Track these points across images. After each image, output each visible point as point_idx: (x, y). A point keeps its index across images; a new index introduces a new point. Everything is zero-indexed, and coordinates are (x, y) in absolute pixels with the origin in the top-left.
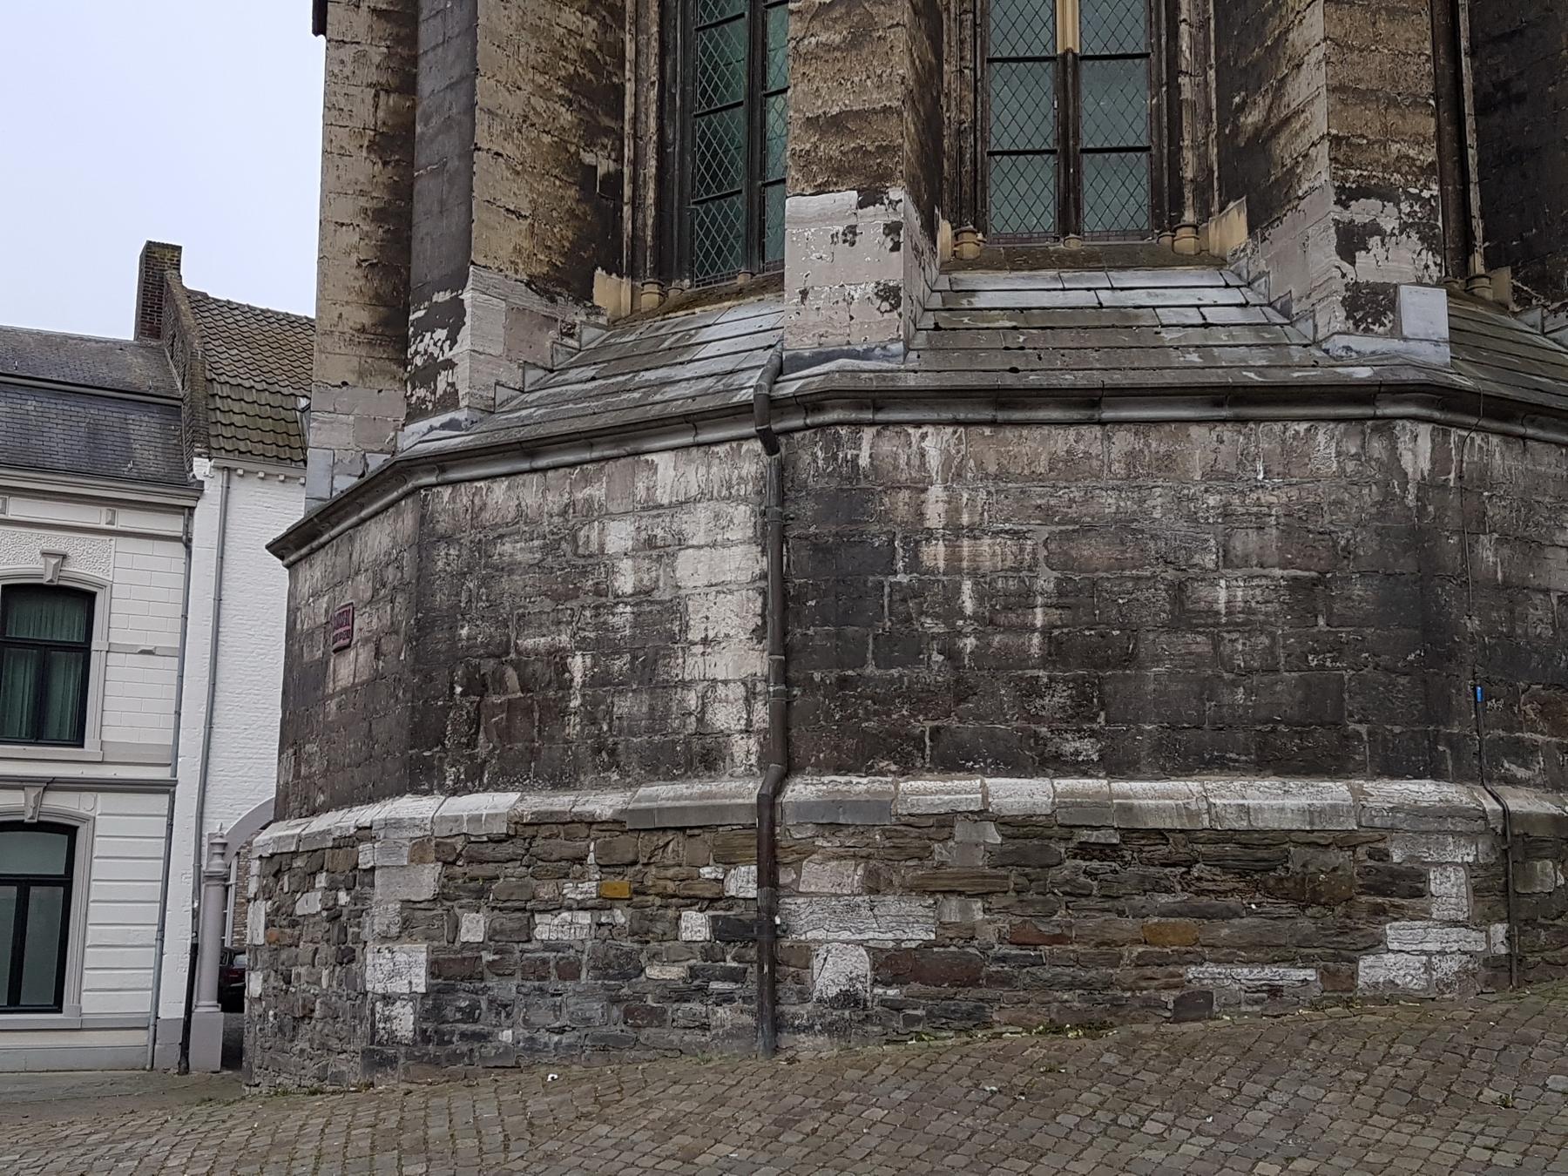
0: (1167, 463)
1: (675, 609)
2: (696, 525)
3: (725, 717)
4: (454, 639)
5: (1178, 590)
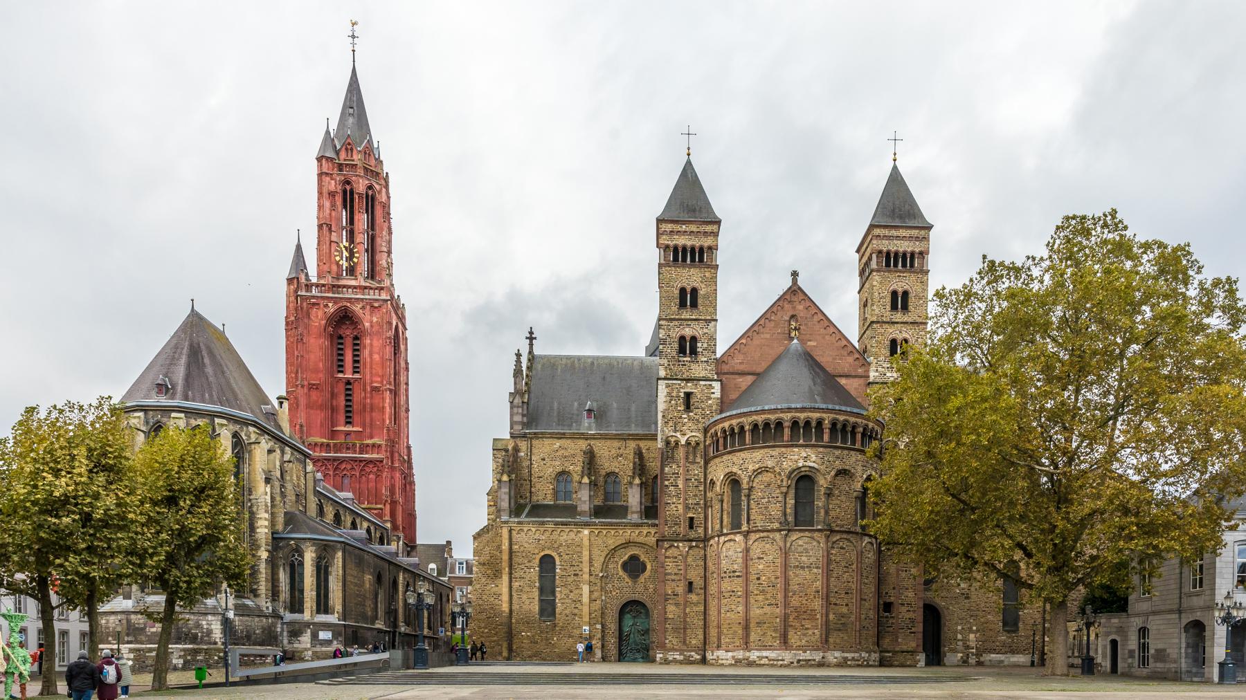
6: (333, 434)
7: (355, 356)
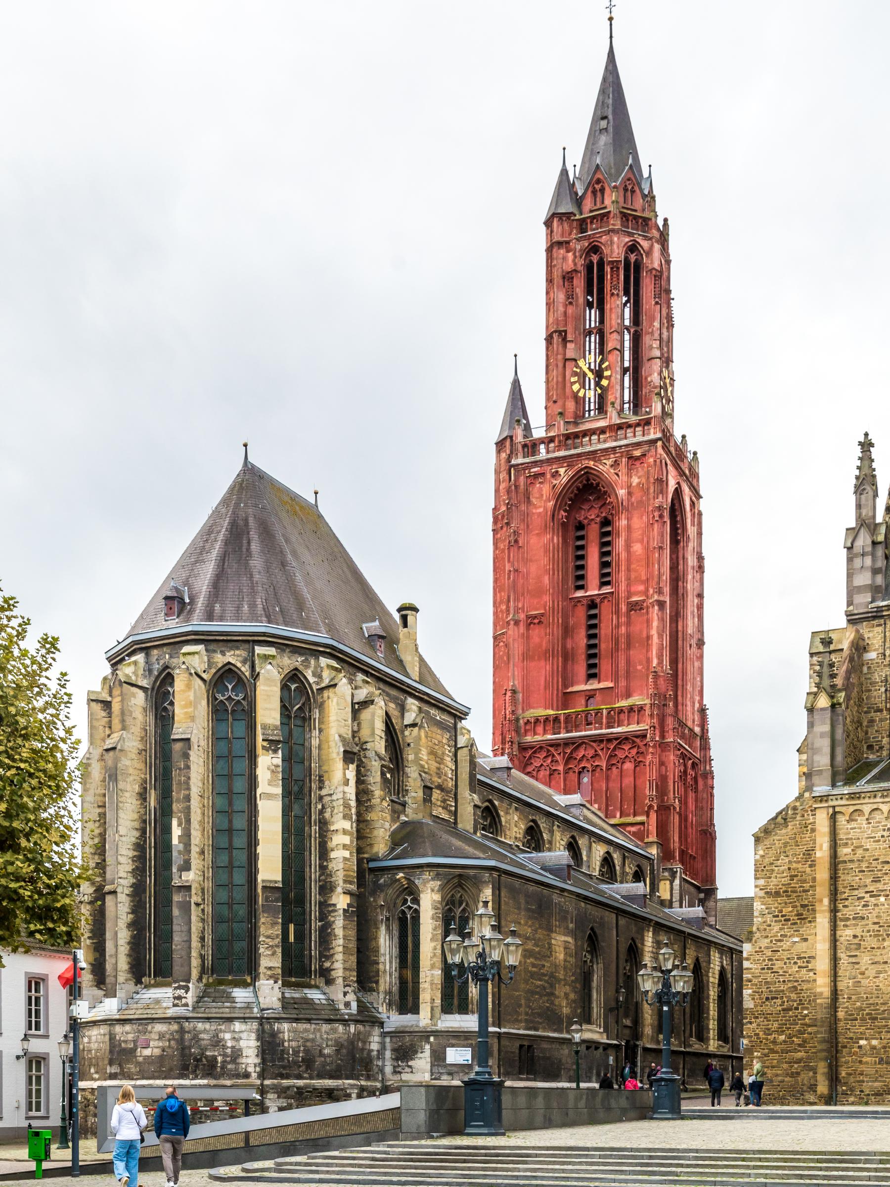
0: (319, 1030)
1: (240, 1050)
2: (244, 1035)
3: (251, 1069)
4: (190, 1051)
5: (320, 1051)
6: (566, 699)
7: (604, 554)
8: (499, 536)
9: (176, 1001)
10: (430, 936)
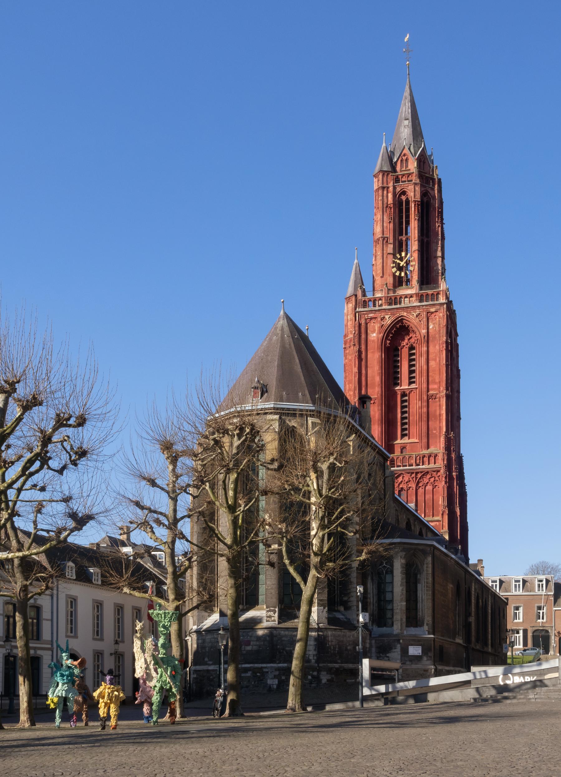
3: (311, 658)
5: (346, 648)
8: (348, 351)
9: (268, 619)
10: (400, 583)
